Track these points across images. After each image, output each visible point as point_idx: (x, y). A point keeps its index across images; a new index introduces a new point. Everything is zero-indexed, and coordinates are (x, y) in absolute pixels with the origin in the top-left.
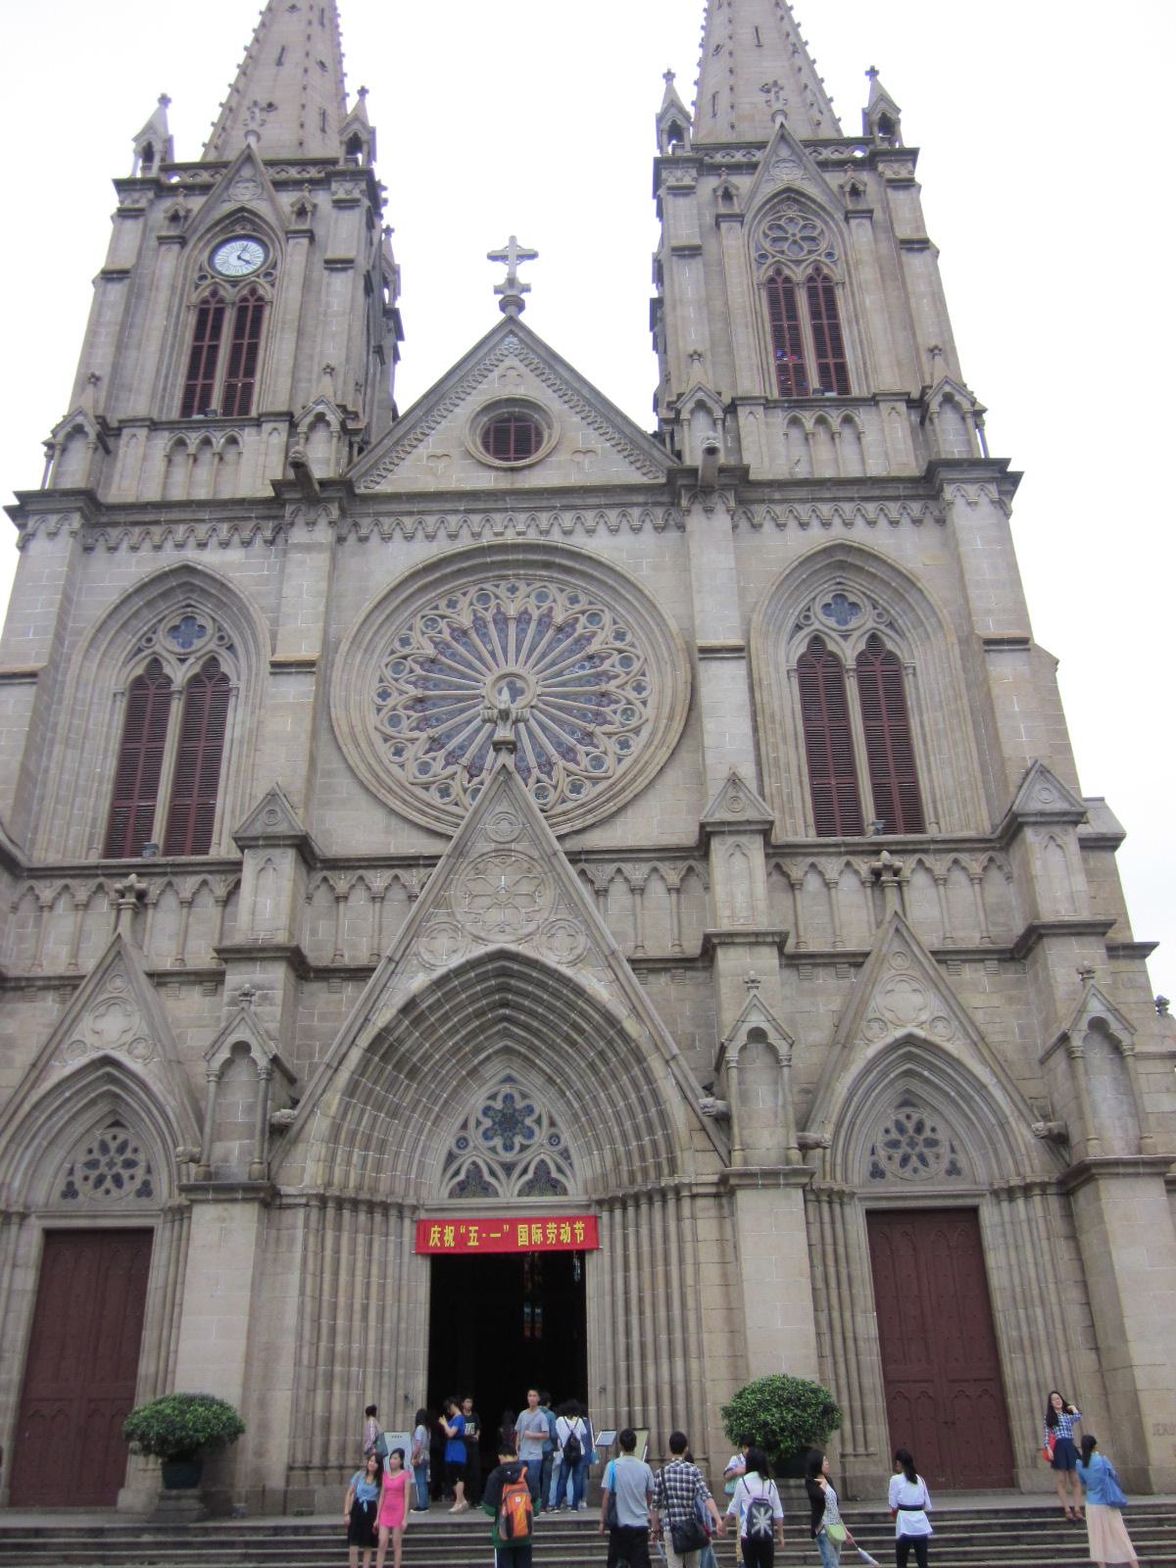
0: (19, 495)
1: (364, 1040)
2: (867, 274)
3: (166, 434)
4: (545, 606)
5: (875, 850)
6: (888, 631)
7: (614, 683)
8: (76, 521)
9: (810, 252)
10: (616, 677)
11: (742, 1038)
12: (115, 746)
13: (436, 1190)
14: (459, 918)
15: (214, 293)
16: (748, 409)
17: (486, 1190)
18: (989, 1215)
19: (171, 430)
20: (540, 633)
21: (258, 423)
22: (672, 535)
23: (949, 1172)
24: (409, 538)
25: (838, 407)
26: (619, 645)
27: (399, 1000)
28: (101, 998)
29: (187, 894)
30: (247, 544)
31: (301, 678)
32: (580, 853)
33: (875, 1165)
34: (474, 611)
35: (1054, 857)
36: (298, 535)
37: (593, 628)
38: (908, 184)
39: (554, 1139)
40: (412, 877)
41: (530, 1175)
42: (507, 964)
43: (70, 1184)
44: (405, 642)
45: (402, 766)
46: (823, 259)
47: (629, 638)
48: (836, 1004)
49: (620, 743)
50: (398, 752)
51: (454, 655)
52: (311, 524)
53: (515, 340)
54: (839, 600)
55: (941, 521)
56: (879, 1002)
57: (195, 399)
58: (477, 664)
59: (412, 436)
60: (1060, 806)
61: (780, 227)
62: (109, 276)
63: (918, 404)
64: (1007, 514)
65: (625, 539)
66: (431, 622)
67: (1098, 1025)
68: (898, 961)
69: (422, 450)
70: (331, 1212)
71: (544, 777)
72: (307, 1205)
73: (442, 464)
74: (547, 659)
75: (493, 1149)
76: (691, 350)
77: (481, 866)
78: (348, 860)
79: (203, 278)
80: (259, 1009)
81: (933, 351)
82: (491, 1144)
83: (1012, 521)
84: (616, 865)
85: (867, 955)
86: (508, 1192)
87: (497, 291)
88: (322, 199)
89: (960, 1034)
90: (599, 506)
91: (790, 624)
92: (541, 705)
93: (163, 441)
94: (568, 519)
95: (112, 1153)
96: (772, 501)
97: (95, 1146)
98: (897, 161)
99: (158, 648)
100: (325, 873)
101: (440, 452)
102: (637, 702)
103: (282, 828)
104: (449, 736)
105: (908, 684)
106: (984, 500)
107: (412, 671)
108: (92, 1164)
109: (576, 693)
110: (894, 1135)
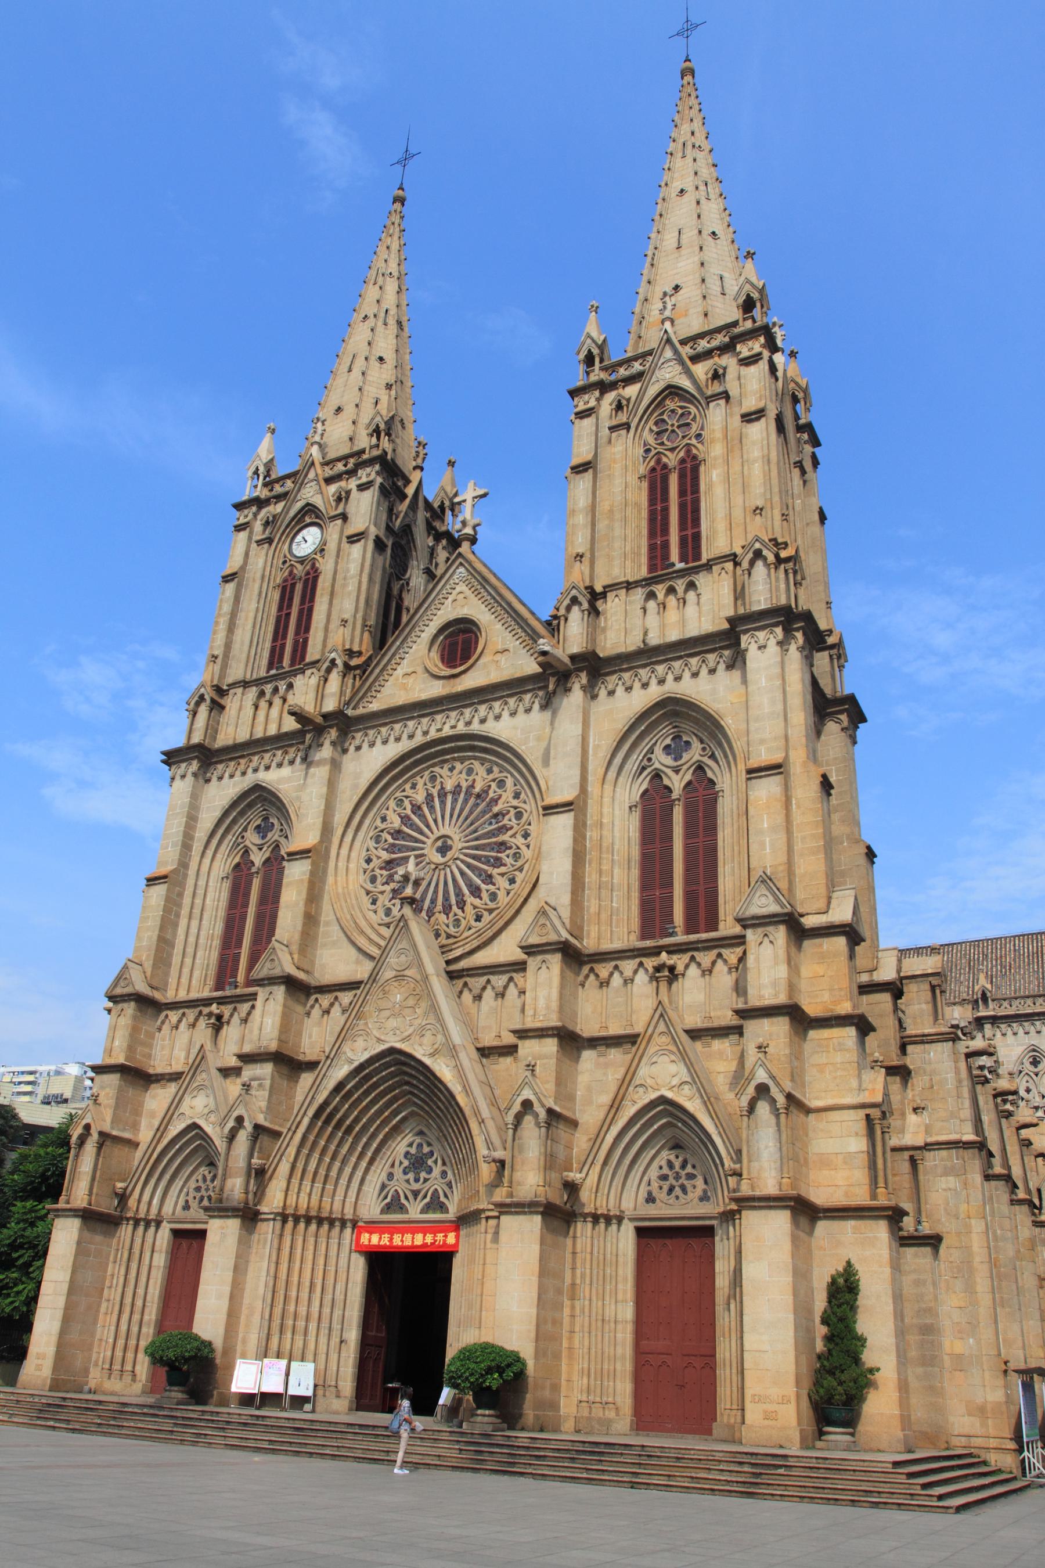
0: (164, 753)
1: (311, 1113)
3: (254, 688)
4: (471, 778)
5: (656, 952)
6: (710, 762)
7: (510, 833)
8: (195, 765)
9: (684, 437)
10: (511, 828)
11: (517, 1107)
12: (222, 913)
13: (371, 1208)
14: (370, 1026)
15: (291, 573)
16: (615, 593)
17: (402, 1209)
19: (256, 685)
20: (466, 801)
23: (701, 1199)
25: (683, 577)
26: (515, 803)
27: (330, 1084)
28: (195, 1085)
29: (243, 1015)
30: (292, 762)
31: (304, 861)
32: (463, 970)
33: (650, 1193)
34: (427, 790)
35: (767, 950)
37: (499, 792)
41: (428, 1199)
42: (398, 1056)
43: (187, 1201)
45: (375, 912)
46: (694, 441)
47: (523, 796)
48: (619, 1075)
49: (510, 880)
50: (374, 902)
51: (413, 826)
53: (462, 569)
54: (677, 740)
57: (276, 657)
58: (426, 830)
59: (393, 661)
60: (774, 908)
61: (663, 421)
66: (400, 802)
68: (665, 1039)
69: (400, 671)
70: (290, 1224)
71: (459, 912)
72: (274, 1220)
73: (410, 680)
74: (468, 821)
75: (408, 1181)
77: (387, 989)
78: (328, 986)
79: (285, 562)
80: (258, 1093)
82: (407, 1177)
84: (485, 978)
85: (637, 1036)
86: (415, 1211)
88: (353, 484)
89: (697, 1095)
90: (503, 697)
92: (462, 857)
93: (252, 692)
94: (483, 709)
95: (208, 1182)
96: (622, 670)
97: (200, 1178)
98: (751, 339)
99: (247, 843)
100: (318, 996)
101: (410, 670)
102: (524, 848)
103: (277, 972)
105: (720, 800)
106: (772, 643)
107: (386, 841)
108: (198, 1189)
109: (484, 845)
110: (666, 1170)
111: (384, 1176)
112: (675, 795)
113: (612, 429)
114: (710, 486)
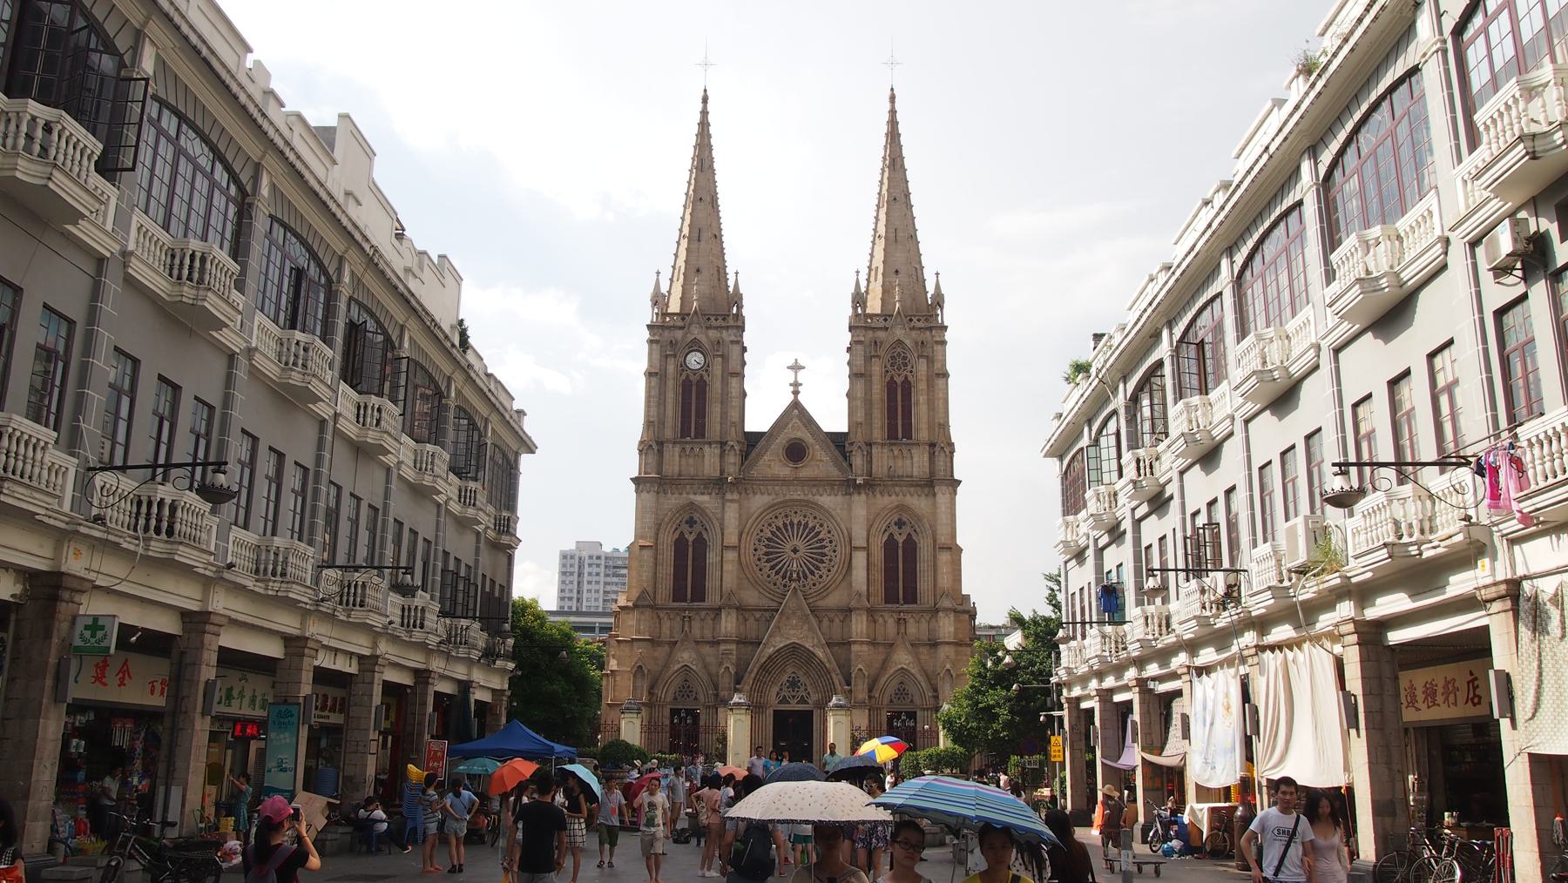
1: (758, 666)
2: (923, 386)
15: (688, 376)
18: (918, 714)
20: (804, 530)
21: (710, 444)
22: (848, 497)
24: (762, 494)
27: (767, 655)
35: (947, 620)
36: (728, 496)
38: (944, 343)
39: (806, 690)
40: (767, 614)
44: (762, 531)
50: (761, 570)
51: (777, 537)
52: (732, 492)
53: (796, 411)
55: (934, 495)
56: (895, 657)
62: (649, 374)
63: (932, 445)
64: (955, 494)
65: (832, 497)
67: (949, 670)
76: (859, 420)
81: (940, 424)
83: (958, 497)
87: (791, 385)
91: (883, 530)
93: (677, 449)
94: (814, 490)
104: (776, 565)
108: (681, 691)
111: (778, 689)
112: (900, 545)
113: (871, 357)
114: (917, 403)
